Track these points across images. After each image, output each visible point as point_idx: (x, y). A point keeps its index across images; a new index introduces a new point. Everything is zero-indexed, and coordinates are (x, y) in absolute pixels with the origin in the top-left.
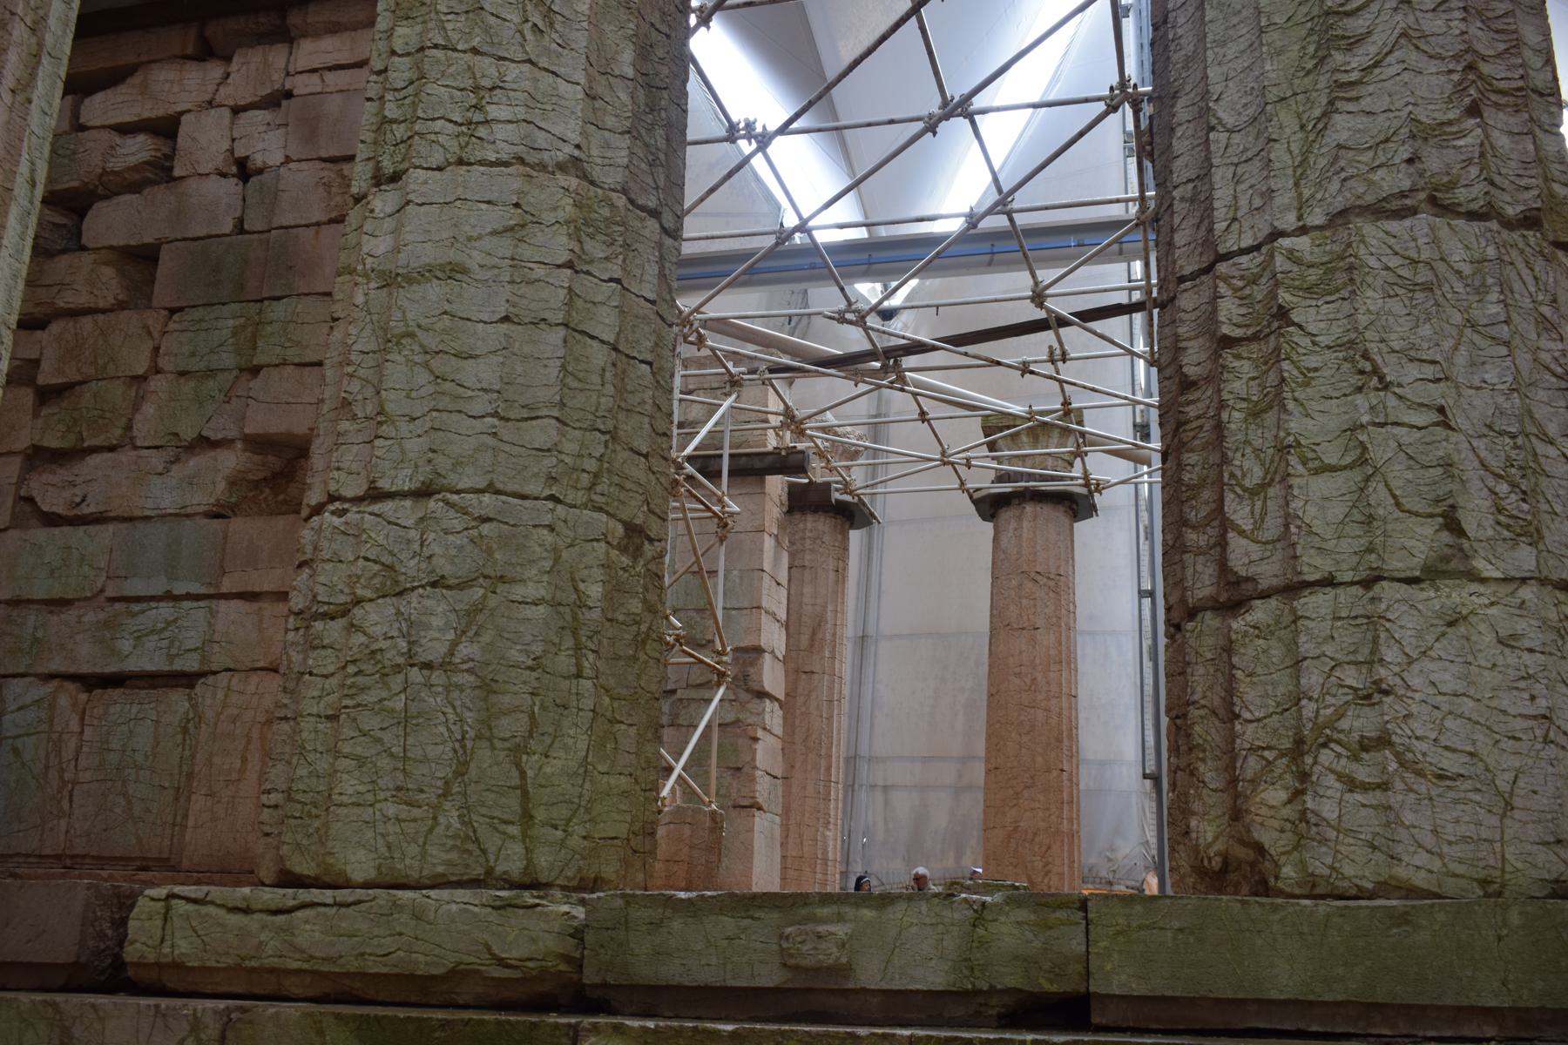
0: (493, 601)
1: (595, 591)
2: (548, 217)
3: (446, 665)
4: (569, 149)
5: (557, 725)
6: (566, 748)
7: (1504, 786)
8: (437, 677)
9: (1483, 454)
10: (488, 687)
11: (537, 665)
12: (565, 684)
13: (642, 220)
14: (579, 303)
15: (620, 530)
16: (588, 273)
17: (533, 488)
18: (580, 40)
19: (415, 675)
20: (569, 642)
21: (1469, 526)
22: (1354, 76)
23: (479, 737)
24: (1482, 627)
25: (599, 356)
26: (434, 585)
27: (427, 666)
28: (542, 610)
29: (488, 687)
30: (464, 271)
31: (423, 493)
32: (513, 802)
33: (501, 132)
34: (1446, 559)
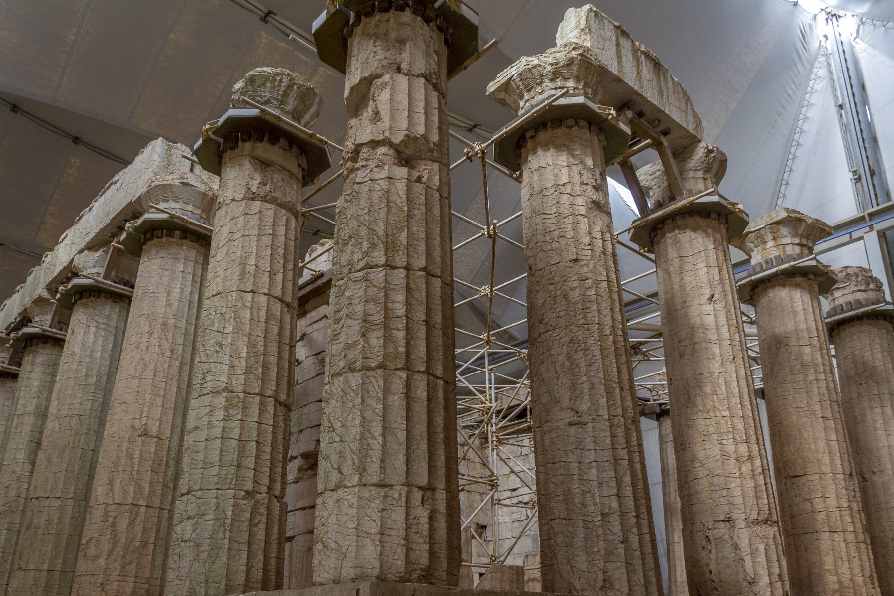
0: (200, 521)
1: (230, 513)
2: (218, 407)
3: (190, 541)
4: (225, 385)
5: (218, 554)
7: (344, 550)
8: (187, 544)
17: (213, 487)
19: (183, 544)
20: (222, 529)
21: (345, 470)
23: (195, 560)
24: (345, 502)
25: (234, 443)
27: (186, 541)
28: (211, 522)
29: (198, 546)
30: (198, 427)
31: (188, 493)
32: (203, 577)
33: (209, 384)
34: (340, 482)
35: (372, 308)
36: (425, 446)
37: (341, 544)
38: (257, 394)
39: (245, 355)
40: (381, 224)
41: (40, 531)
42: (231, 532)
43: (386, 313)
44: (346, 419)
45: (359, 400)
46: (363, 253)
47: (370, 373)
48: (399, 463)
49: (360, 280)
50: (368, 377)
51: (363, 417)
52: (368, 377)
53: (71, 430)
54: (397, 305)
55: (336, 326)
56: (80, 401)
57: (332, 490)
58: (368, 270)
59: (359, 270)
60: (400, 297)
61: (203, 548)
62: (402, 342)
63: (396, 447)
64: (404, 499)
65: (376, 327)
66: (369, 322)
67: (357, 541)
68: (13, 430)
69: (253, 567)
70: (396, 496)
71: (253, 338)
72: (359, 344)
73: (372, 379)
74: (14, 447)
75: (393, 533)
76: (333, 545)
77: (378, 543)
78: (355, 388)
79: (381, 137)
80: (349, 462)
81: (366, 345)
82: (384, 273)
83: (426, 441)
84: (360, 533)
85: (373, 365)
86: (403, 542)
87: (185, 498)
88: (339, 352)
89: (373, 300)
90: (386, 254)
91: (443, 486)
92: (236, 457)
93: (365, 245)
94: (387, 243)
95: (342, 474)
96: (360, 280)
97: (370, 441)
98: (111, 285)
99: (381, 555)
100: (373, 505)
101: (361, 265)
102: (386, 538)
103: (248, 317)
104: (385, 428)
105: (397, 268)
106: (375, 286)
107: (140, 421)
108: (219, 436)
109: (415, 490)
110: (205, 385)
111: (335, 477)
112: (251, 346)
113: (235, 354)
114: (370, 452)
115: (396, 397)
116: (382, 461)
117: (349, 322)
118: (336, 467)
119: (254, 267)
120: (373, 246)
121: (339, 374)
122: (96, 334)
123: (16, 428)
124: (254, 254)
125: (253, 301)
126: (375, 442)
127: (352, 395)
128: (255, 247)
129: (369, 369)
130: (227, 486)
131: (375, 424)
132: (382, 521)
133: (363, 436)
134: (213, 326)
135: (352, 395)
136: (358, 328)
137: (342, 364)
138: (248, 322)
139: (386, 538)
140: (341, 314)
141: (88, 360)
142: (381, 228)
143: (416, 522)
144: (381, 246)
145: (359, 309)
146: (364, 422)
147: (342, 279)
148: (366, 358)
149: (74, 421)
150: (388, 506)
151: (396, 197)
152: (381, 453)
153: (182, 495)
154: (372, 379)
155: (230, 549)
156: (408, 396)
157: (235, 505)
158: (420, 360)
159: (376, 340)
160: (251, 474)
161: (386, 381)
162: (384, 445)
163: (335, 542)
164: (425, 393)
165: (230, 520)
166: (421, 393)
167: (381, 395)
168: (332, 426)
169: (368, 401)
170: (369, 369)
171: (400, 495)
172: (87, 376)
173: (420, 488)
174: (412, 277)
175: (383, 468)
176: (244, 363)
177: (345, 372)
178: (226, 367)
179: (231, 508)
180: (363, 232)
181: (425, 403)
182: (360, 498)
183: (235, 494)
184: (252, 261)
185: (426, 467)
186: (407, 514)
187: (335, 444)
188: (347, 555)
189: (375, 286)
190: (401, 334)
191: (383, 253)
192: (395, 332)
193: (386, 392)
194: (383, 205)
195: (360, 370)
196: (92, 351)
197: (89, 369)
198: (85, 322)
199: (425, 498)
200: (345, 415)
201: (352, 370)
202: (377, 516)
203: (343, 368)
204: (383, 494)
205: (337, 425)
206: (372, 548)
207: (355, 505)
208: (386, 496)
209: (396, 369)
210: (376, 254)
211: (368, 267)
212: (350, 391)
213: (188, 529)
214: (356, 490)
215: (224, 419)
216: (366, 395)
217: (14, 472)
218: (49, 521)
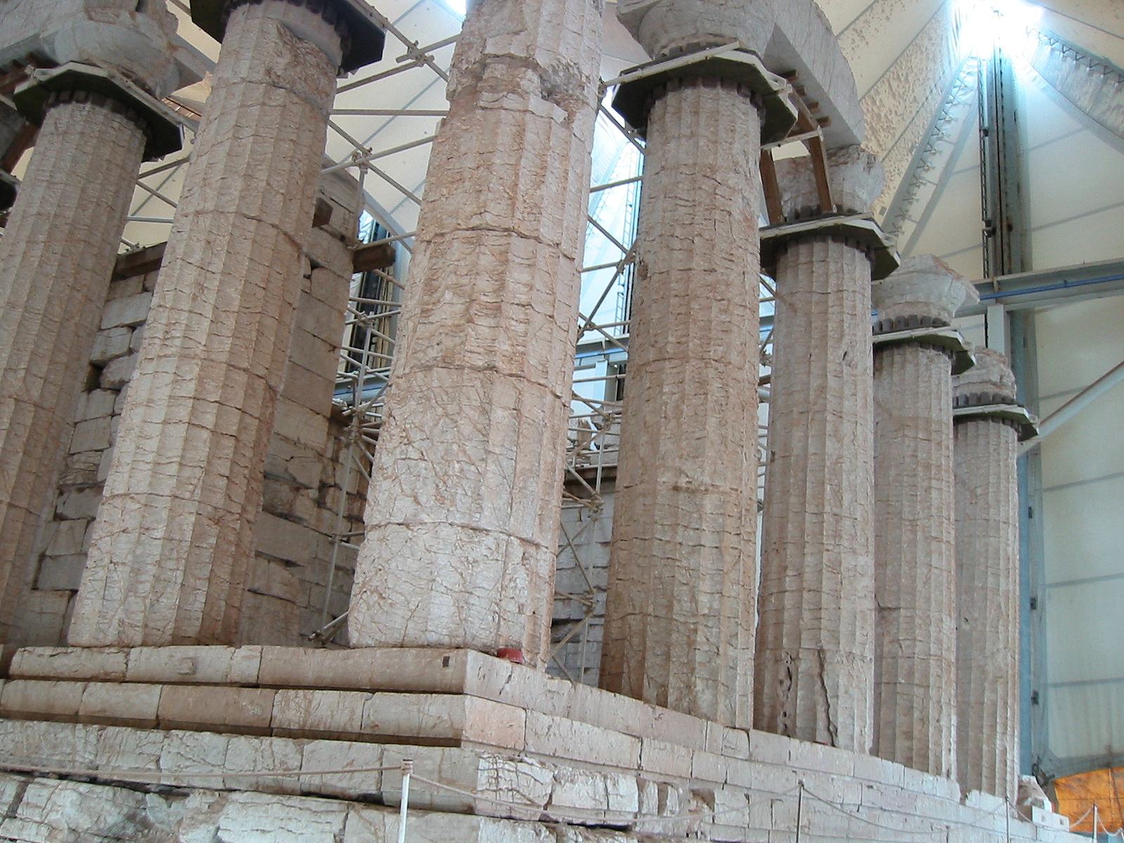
8: (120, 568)
9: (438, 469)
10: (136, 572)
11: (158, 563)
16: (204, 399)
18: (211, 298)
21: (423, 499)
22: (430, 307)
24: (421, 544)
25: (205, 435)
26: (124, 531)
28: (160, 542)
29: (136, 572)
38: (244, 370)
57: (399, 524)
61: (143, 578)
87: (118, 502)
88: (427, 334)
95: (418, 503)
109: (516, 542)
114: (464, 482)
126: (473, 468)
135: (445, 398)
143: (512, 584)
153: (114, 497)
155: (182, 585)
184: (263, 176)
205: (416, 436)
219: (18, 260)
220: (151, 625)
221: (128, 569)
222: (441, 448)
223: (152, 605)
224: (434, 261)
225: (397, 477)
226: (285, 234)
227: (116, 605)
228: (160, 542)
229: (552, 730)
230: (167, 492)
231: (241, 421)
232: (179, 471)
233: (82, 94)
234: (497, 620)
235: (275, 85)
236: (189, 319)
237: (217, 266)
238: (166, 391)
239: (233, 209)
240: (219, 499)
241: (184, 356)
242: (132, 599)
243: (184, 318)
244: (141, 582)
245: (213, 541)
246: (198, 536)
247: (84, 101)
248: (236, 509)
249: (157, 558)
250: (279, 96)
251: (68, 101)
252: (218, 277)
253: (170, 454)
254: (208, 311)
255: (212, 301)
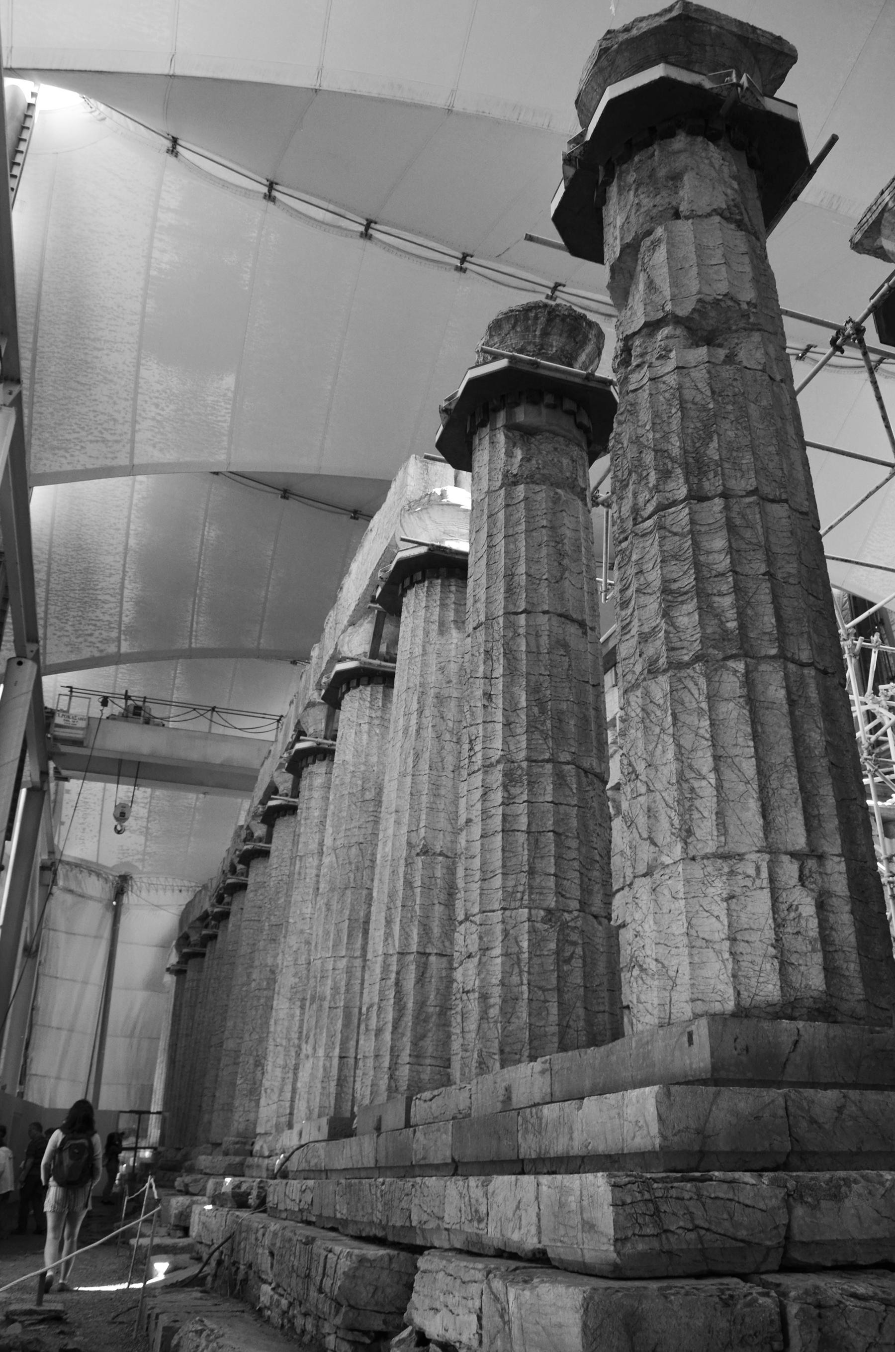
1: (525, 944)
3: (473, 990)
4: (500, 753)
5: (514, 1008)
6: (518, 1018)
7: (672, 973)
8: (471, 996)
9: (667, 798)
10: (484, 997)
11: (502, 983)
12: (515, 990)
13: (542, 767)
14: (510, 818)
15: (542, 913)
18: (499, 701)
19: (465, 997)
20: (516, 970)
21: (659, 840)
23: (482, 1018)
24: (666, 892)
25: (522, 838)
26: (469, 957)
27: (468, 992)
29: (484, 997)
35: (675, 569)
36: (795, 780)
37: (666, 963)
39: (524, 704)
40: (675, 441)
41: (326, 1005)
42: (529, 973)
43: (698, 572)
44: (652, 754)
45: (670, 719)
46: (651, 491)
47: (683, 674)
48: (750, 814)
49: (651, 532)
50: (680, 680)
51: (679, 746)
52: (680, 680)
53: (350, 863)
54: (716, 556)
55: (623, 613)
56: (357, 824)
58: (662, 513)
59: (649, 517)
60: (719, 542)
62: (731, 614)
63: (742, 787)
64: (765, 874)
65: (686, 597)
66: (671, 592)
67: (691, 955)
68: (296, 876)
69: (568, 1026)
70: (751, 871)
71: (533, 678)
72: (660, 631)
73: (691, 685)
74: (299, 898)
75: (754, 937)
76: (653, 966)
77: (726, 955)
78: (661, 702)
79: (661, 315)
80: (664, 823)
81: (671, 629)
82: (687, 510)
83: (794, 772)
84: (695, 942)
85: (686, 658)
86: (772, 951)
89: (675, 557)
90: (687, 481)
91: (838, 850)
92: (525, 858)
93: (653, 479)
94: (687, 464)
95: (655, 845)
96: (651, 532)
97: (696, 784)
98: (380, 666)
99: (734, 976)
100: (711, 890)
101: (650, 508)
102: (741, 947)
103: (523, 648)
104: (717, 758)
105: (708, 499)
106: (675, 534)
107: (418, 835)
108: (500, 828)
109: (786, 859)
110: (474, 759)
111: (646, 853)
112: (534, 690)
113: (511, 708)
115: (731, 705)
116: (720, 814)
117: (643, 600)
118: (645, 835)
119: (524, 577)
120: (665, 475)
121: (635, 686)
122: (369, 733)
123: (300, 874)
124: (523, 561)
125: (528, 625)
126: (704, 783)
127: (659, 713)
128: (523, 549)
129: (680, 666)
130: (518, 904)
131: (700, 753)
132: (729, 915)
133: (681, 778)
134: (477, 671)
135: (659, 713)
136: (656, 606)
137: (638, 669)
138: (524, 657)
139: (741, 947)
140: (629, 592)
141: (363, 768)
142: (675, 446)
143: (792, 915)
144: (679, 471)
145: (654, 577)
146: (681, 754)
147: (626, 539)
148: (673, 649)
149: (354, 851)
150: (738, 890)
151: (694, 392)
152: (715, 799)
154: (691, 685)
155: (530, 1000)
156: (752, 701)
157: (532, 931)
158: (767, 638)
159: (687, 617)
160: (551, 882)
161: (709, 680)
162: (719, 787)
163: (656, 960)
164: (783, 692)
165: (526, 955)
166: (776, 693)
167: (704, 705)
168: (634, 771)
169: (683, 717)
170: (680, 666)
171: (758, 869)
172: (363, 789)
173: (793, 855)
174: (736, 508)
175: (722, 826)
176: (524, 717)
177: (645, 679)
178: (499, 727)
179: (526, 936)
180: (649, 458)
181: (785, 708)
182: (687, 881)
183: (530, 913)
184: (522, 569)
185: (801, 817)
186: (775, 900)
187: (639, 799)
188: (678, 981)
189: (675, 534)
190: (727, 601)
191: (682, 481)
192: (716, 599)
193: (712, 698)
194: (673, 411)
195: (665, 671)
196: (367, 755)
197: (365, 780)
198: (355, 719)
199: (806, 872)
200: (651, 748)
201: (652, 670)
202: (720, 909)
203: (641, 673)
204: (726, 869)
206: (718, 965)
207: (681, 895)
208: (732, 873)
209: (726, 658)
210: (671, 485)
211: (661, 508)
212: (655, 709)
213: (470, 972)
214: (680, 869)
215: (503, 804)
216: (679, 708)
217: (302, 932)
218: (335, 989)
219: (400, 733)
220: (507, 1049)
221: (477, 995)
222: (665, 772)
223: (504, 1029)
224: (623, 570)
225: (632, 822)
226: (560, 615)
227: (474, 1035)
228: (499, 960)
229: (846, 1112)
230: (497, 906)
231: (556, 813)
232: (504, 879)
233: (419, 576)
234: (777, 967)
235: (515, 484)
236: (485, 729)
237: (499, 671)
238: (479, 806)
239: (501, 612)
240: (551, 901)
241: (487, 767)
242: (485, 1026)
243: (481, 727)
244: (491, 1006)
245: (553, 946)
246: (536, 944)
247: (423, 581)
248: (574, 905)
249: (500, 977)
250: (521, 490)
251: (412, 585)
252: (501, 679)
253: (492, 868)
254: (499, 717)
255: (501, 706)
